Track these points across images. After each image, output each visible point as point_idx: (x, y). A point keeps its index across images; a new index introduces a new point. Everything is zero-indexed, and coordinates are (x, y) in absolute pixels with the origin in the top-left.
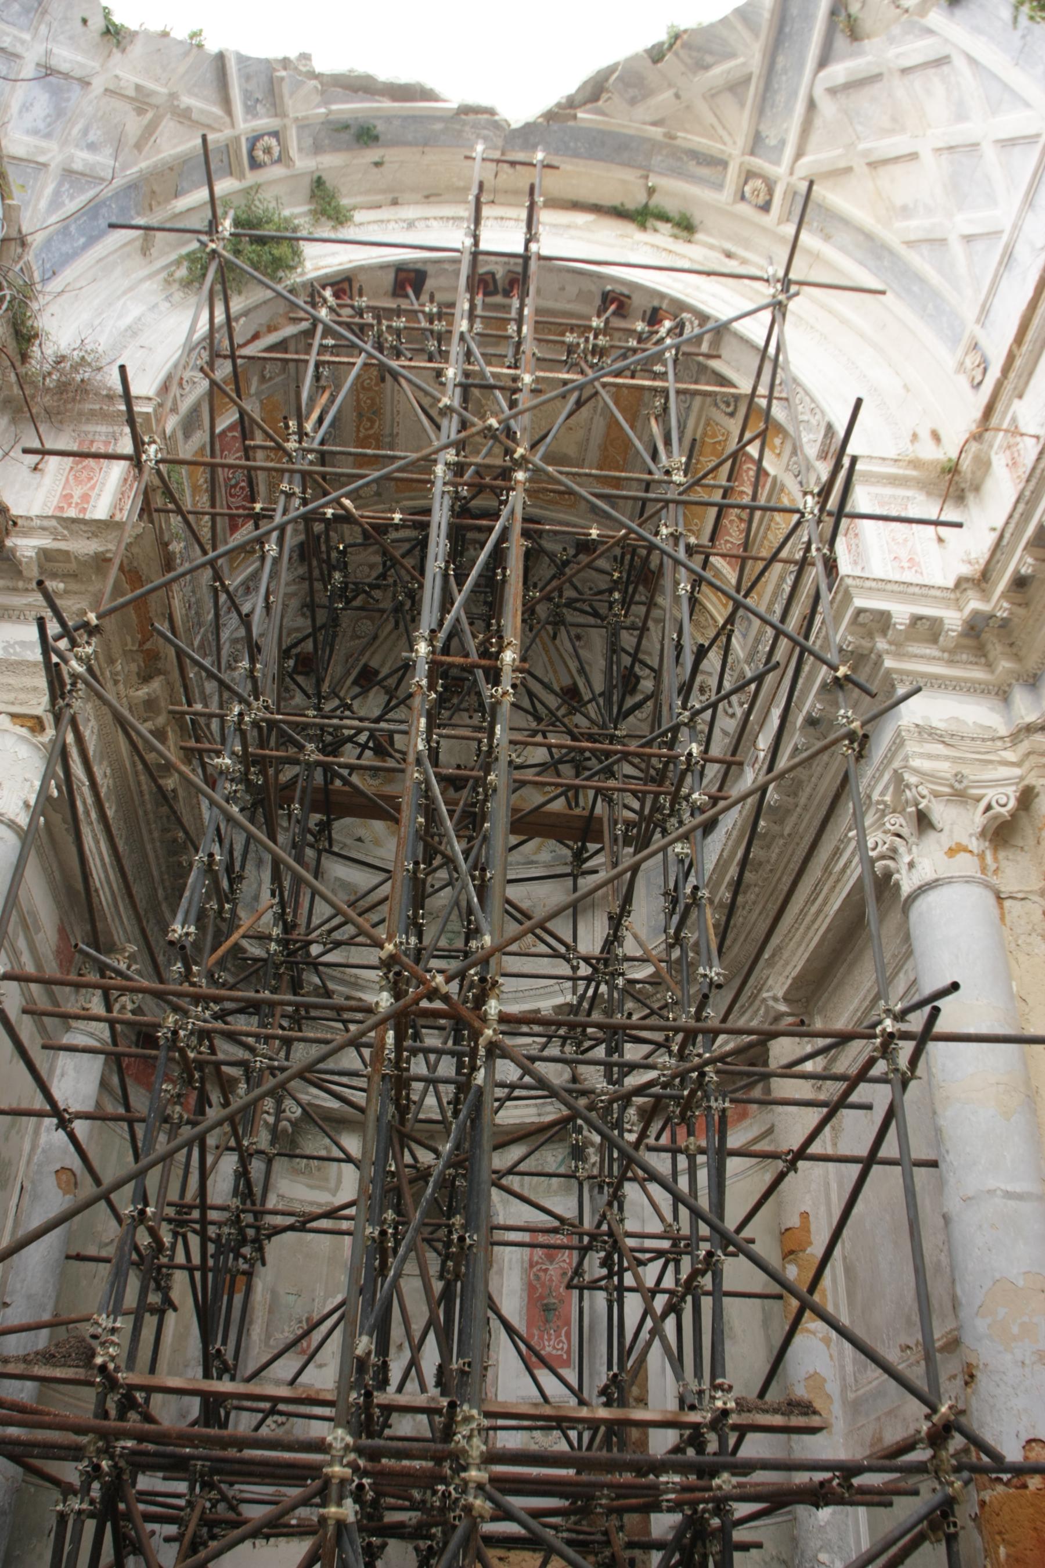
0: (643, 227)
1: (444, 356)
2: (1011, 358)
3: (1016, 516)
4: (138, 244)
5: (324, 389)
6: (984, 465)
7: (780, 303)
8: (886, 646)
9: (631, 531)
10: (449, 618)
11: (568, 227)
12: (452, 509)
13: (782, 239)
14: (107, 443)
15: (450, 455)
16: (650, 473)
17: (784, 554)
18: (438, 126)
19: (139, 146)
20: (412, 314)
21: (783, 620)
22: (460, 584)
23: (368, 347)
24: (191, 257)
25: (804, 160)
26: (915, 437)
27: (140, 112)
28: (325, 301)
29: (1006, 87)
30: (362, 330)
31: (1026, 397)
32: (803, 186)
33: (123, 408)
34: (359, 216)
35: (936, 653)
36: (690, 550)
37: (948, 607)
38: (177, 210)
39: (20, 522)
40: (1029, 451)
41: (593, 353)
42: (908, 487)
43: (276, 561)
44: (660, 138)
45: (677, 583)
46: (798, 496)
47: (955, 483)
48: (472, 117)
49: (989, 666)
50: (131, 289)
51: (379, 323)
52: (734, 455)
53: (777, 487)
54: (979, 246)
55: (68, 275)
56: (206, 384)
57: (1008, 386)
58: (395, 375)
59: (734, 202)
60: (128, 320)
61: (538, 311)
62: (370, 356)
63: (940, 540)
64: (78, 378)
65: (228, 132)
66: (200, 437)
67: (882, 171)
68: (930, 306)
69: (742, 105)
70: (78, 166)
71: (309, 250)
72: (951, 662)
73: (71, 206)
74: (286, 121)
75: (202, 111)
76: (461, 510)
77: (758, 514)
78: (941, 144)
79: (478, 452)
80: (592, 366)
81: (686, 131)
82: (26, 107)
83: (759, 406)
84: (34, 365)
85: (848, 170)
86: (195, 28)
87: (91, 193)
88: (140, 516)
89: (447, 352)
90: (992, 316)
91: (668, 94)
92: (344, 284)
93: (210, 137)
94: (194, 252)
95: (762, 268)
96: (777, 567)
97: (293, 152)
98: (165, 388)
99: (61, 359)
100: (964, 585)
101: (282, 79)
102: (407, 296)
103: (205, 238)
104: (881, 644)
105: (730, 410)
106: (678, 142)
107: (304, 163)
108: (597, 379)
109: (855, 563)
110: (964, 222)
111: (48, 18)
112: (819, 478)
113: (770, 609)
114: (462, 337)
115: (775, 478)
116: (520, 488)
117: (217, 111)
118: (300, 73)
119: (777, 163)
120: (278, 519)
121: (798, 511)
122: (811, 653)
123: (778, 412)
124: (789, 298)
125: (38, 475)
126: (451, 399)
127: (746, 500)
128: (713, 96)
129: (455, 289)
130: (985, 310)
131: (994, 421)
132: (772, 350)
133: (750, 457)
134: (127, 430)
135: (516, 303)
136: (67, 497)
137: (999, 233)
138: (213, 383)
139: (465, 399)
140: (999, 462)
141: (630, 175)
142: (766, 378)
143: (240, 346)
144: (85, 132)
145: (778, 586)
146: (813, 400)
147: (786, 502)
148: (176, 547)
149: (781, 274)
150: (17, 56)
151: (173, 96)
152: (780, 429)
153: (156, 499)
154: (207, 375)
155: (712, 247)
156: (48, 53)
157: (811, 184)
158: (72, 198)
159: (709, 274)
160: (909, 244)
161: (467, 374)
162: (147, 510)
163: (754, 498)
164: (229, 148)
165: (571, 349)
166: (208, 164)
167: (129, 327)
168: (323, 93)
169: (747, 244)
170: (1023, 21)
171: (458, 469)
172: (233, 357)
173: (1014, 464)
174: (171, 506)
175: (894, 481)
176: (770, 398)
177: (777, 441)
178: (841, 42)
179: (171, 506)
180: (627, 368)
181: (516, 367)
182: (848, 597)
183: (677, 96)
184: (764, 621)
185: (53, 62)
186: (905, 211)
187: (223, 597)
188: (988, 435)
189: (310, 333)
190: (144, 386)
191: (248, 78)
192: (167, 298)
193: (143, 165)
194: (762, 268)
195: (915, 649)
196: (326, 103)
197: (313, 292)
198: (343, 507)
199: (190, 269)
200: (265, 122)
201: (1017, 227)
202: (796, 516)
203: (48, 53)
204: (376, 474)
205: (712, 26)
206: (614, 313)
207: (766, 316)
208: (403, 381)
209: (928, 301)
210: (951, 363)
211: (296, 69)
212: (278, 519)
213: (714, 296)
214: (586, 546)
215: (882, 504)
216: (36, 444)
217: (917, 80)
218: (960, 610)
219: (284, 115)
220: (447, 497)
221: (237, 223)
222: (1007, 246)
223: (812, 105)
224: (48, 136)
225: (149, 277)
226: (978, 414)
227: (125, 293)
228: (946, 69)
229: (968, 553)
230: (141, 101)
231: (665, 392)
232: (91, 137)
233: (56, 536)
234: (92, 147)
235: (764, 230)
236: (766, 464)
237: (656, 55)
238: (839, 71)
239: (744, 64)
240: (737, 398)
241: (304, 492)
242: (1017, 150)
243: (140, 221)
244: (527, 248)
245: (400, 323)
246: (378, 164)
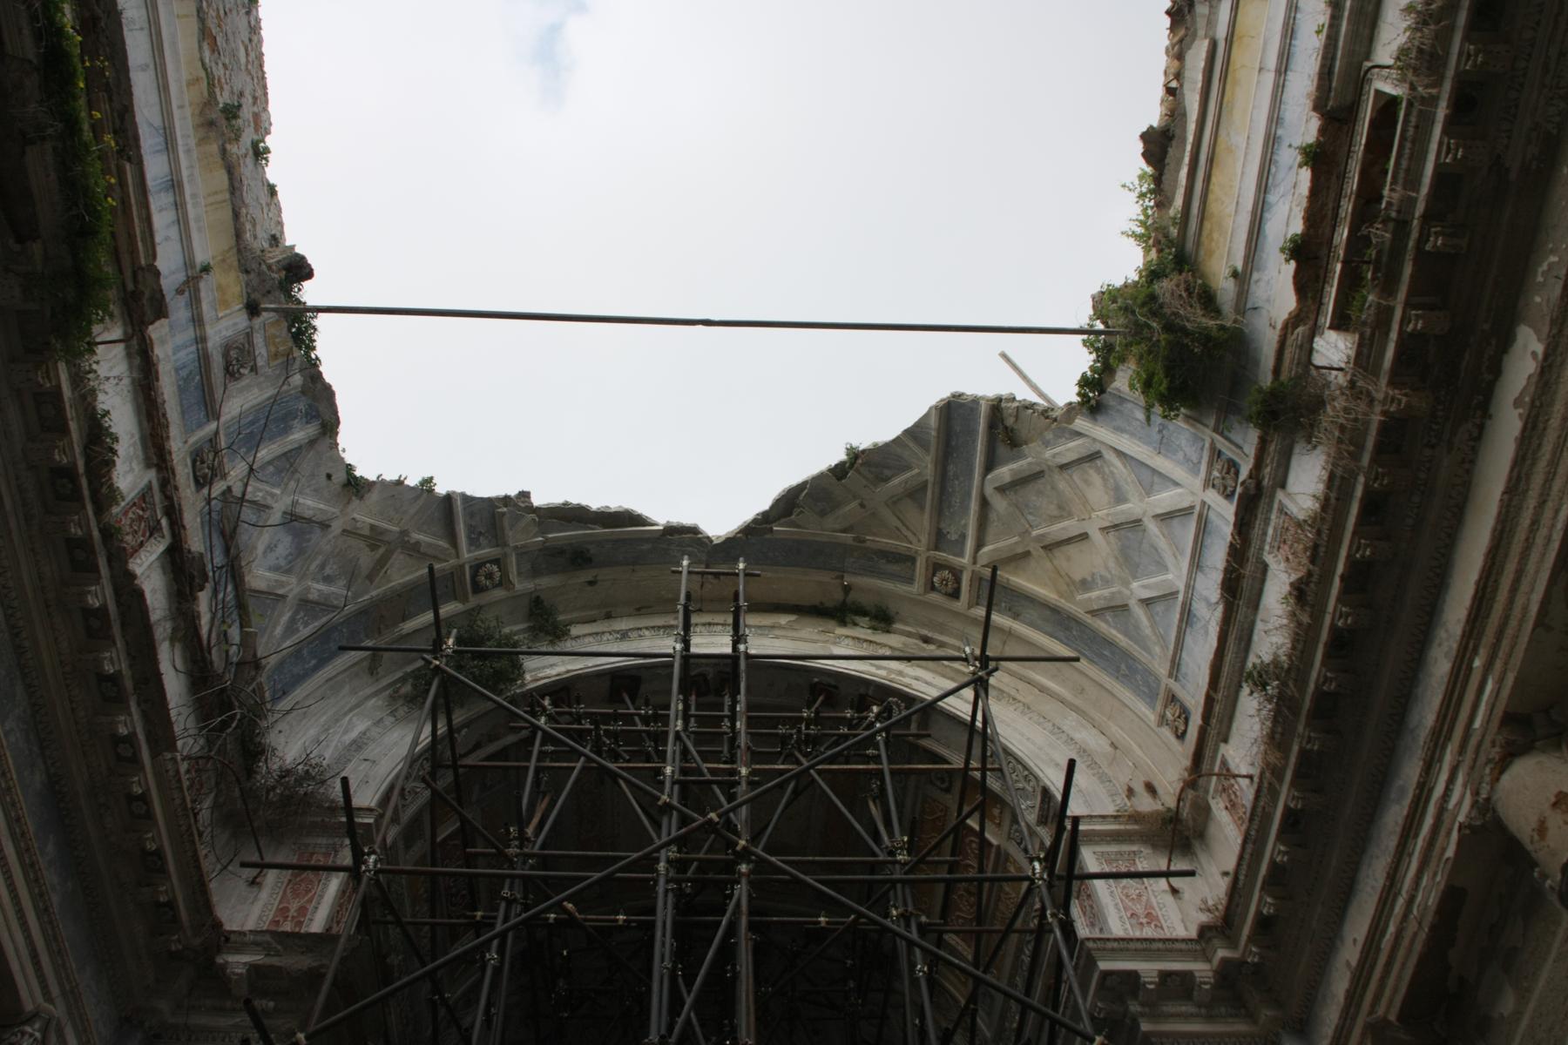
0: (843, 623)
1: (662, 756)
2: (1209, 701)
3: (1247, 856)
4: (365, 664)
5: (544, 794)
6: (1204, 811)
7: (981, 678)
8: (1139, 1009)
9: (860, 915)
10: (680, 1020)
11: (773, 627)
12: (676, 906)
13: (974, 621)
14: (327, 855)
15: (673, 852)
16: (874, 854)
17: (1018, 924)
18: (646, 547)
19: (370, 577)
20: (628, 719)
21: (1028, 991)
22: (689, 985)
23: (587, 751)
24: (416, 675)
25: (985, 549)
26: (1130, 792)
27: (373, 548)
28: (544, 709)
29: (1154, 471)
30: (580, 736)
31: (1231, 741)
32: (988, 572)
33: (344, 819)
34: (575, 630)
35: (1192, 1010)
36: (923, 930)
37: (1195, 960)
38: (404, 632)
39: (233, 937)
40: (1246, 792)
41: (807, 743)
42: (1132, 842)
43: (498, 971)
44: (850, 542)
45: (912, 966)
46: (1024, 862)
47: (1177, 833)
48: (676, 537)
49: (1251, 1017)
50: (357, 706)
51: (597, 728)
52: (955, 829)
53: (1002, 857)
54: (1159, 608)
55: (298, 694)
56: (428, 793)
57: (1213, 732)
58: (614, 776)
59: (926, 592)
60: (354, 735)
61: (750, 707)
62: (589, 759)
63: (1175, 891)
64: (302, 791)
65: (453, 562)
66: (421, 847)
67: (1057, 552)
68: (1123, 666)
69: (922, 508)
70: (313, 596)
71: (530, 663)
72: (1210, 1018)
73: (305, 632)
74: (507, 550)
75: (430, 545)
76: (684, 906)
77: (986, 885)
78: (1107, 524)
79: (699, 849)
80: (806, 755)
81: (875, 534)
82: (270, 548)
83: (974, 779)
84: (260, 780)
85: (1027, 554)
86: (427, 475)
87: (324, 620)
88: (358, 927)
89: (665, 752)
90: (1183, 669)
91: (854, 504)
92: (562, 690)
93: (437, 566)
94: (419, 669)
95: (959, 649)
96: (1014, 937)
97: (513, 576)
98: (385, 799)
99: (285, 773)
100: (1209, 934)
101: (503, 514)
102: (623, 701)
103: (428, 657)
104: (1134, 1007)
105: (945, 785)
106: (868, 544)
107: (522, 585)
108: (812, 767)
109: (1093, 925)
110: (1140, 588)
111: (297, 476)
112: (1042, 843)
113: (1011, 983)
114: (678, 736)
115: (998, 847)
116: (744, 880)
117: (443, 544)
118: (520, 509)
119: (961, 555)
120: (499, 928)
121: (1027, 878)
122: (1063, 1025)
123: (993, 783)
124: (989, 674)
125: (255, 889)
126: (670, 796)
127: (972, 874)
128: (895, 503)
129: (669, 692)
130: (1175, 666)
131: (1205, 767)
132: (979, 724)
133: (971, 829)
134: (347, 841)
135: (727, 701)
136: (283, 911)
137: (1175, 594)
138: (434, 792)
139: (684, 798)
140: (1218, 807)
141: (826, 577)
142: (977, 751)
143: (463, 756)
144: (322, 567)
145: (1017, 957)
146: (1025, 768)
147: (1013, 871)
148: (394, 960)
149: (978, 652)
150: (268, 507)
151: (404, 533)
152: (997, 799)
153: (373, 904)
154: (428, 785)
155: (909, 635)
156: (295, 504)
157: (995, 569)
158: (306, 625)
159: (909, 659)
160: (1093, 613)
161: (684, 771)
162: (364, 923)
163: (981, 870)
164: (454, 576)
165: (784, 740)
166: (433, 590)
167: (354, 741)
168: (540, 524)
169: (942, 629)
170: (1157, 420)
171: (679, 865)
172: (455, 767)
173: (1232, 807)
174: (389, 918)
175: (1116, 837)
176: (984, 770)
177: (996, 812)
178: (1002, 450)
179: (389, 918)
180: (840, 753)
181: (733, 762)
182: (1091, 962)
183: (862, 505)
184: (1007, 995)
185: (298, 510)
186: (1085, 585)
187: (442, 1012)
188: (1202, 781)
189: (530, 741)
190: (365, 797)
191: (472, 515)
192: (392, 713)
193: (374, 593)
194: (959, 649)
195: (1170, 1008)
196: (543, 532)
197: (532, 700)
198: (565, 911)
199: (415, 686)
200: (486, 552)
201: (1189, 587)
202: (1025, 884)
203: (295, 504)
204: (597, 875)
205: (887, 445)
206: (823, 703)
207: (968, 693)
208: (622, 782)
209: (1123, 664)
210: (1152, 717)
211: (516, 505)
212: (499, 928)
213: (917, 679)
214: (819, 934)
215: (1109, 862)
216: (255, 858)
217: (1076, 475)
218: (1209, 961)
219: (505, 545)
220: (670, 895)
221: (459, 641)
222: (1184, 604)
223: (984, 503)
224: (288, 572)
225: (375, 694)
226: (1187, 763)
227: (351, 710)
228: (1098, 462)
229: (1205, 901)
230: (375, 538)
231: (881, 772)
232: (328, 571)
233: (268, 950)
234: (328, 580)
235: (956, 614)
236: (987, 835)
237: (839, 471)
238: (1004, 472)
239: (919, 474)
240: (951, 772)
241: (525, 897)
242: (1175, 522)
243: (369, 643)
244: (735, 648)
245: (620, 726)
246: (591, 583)
